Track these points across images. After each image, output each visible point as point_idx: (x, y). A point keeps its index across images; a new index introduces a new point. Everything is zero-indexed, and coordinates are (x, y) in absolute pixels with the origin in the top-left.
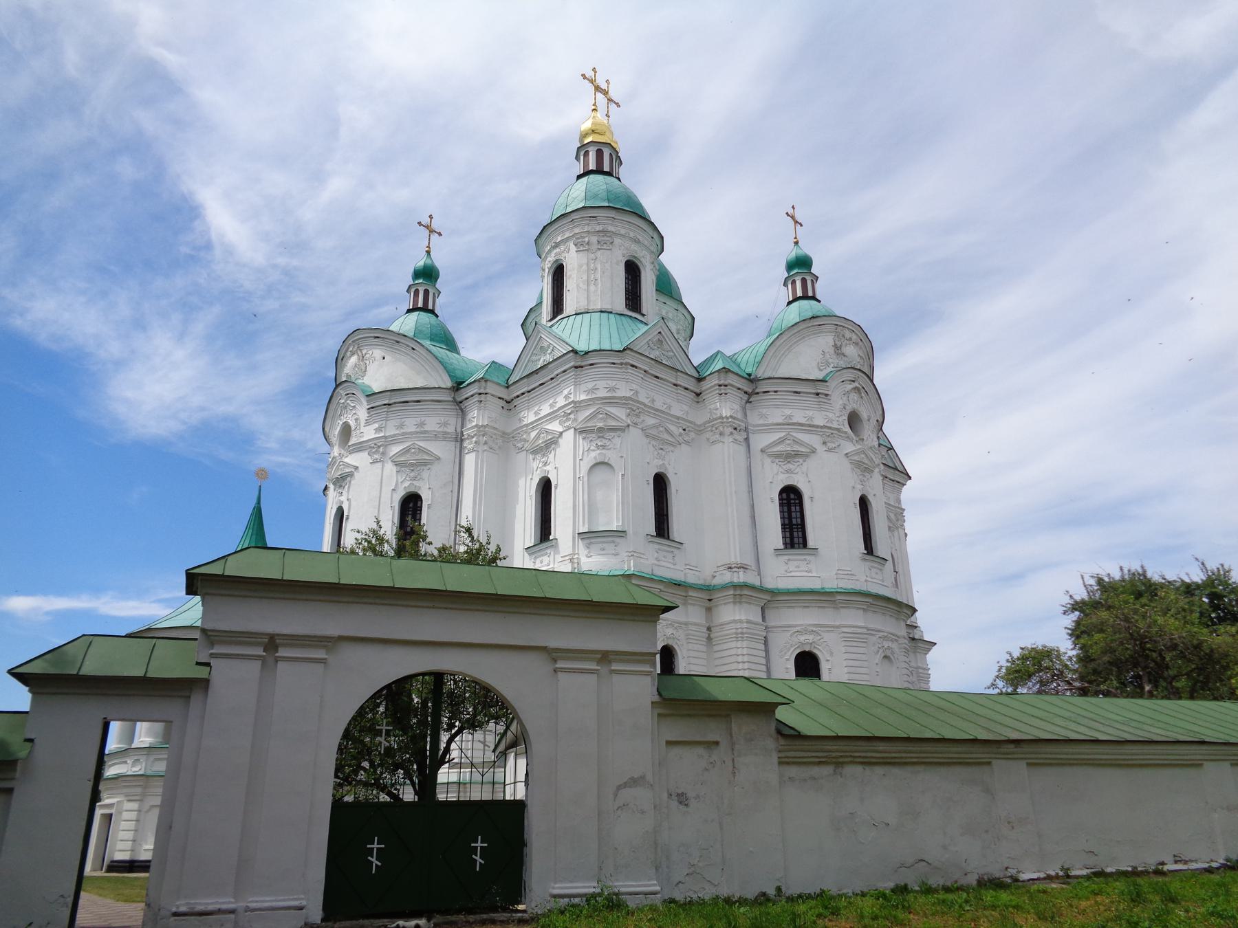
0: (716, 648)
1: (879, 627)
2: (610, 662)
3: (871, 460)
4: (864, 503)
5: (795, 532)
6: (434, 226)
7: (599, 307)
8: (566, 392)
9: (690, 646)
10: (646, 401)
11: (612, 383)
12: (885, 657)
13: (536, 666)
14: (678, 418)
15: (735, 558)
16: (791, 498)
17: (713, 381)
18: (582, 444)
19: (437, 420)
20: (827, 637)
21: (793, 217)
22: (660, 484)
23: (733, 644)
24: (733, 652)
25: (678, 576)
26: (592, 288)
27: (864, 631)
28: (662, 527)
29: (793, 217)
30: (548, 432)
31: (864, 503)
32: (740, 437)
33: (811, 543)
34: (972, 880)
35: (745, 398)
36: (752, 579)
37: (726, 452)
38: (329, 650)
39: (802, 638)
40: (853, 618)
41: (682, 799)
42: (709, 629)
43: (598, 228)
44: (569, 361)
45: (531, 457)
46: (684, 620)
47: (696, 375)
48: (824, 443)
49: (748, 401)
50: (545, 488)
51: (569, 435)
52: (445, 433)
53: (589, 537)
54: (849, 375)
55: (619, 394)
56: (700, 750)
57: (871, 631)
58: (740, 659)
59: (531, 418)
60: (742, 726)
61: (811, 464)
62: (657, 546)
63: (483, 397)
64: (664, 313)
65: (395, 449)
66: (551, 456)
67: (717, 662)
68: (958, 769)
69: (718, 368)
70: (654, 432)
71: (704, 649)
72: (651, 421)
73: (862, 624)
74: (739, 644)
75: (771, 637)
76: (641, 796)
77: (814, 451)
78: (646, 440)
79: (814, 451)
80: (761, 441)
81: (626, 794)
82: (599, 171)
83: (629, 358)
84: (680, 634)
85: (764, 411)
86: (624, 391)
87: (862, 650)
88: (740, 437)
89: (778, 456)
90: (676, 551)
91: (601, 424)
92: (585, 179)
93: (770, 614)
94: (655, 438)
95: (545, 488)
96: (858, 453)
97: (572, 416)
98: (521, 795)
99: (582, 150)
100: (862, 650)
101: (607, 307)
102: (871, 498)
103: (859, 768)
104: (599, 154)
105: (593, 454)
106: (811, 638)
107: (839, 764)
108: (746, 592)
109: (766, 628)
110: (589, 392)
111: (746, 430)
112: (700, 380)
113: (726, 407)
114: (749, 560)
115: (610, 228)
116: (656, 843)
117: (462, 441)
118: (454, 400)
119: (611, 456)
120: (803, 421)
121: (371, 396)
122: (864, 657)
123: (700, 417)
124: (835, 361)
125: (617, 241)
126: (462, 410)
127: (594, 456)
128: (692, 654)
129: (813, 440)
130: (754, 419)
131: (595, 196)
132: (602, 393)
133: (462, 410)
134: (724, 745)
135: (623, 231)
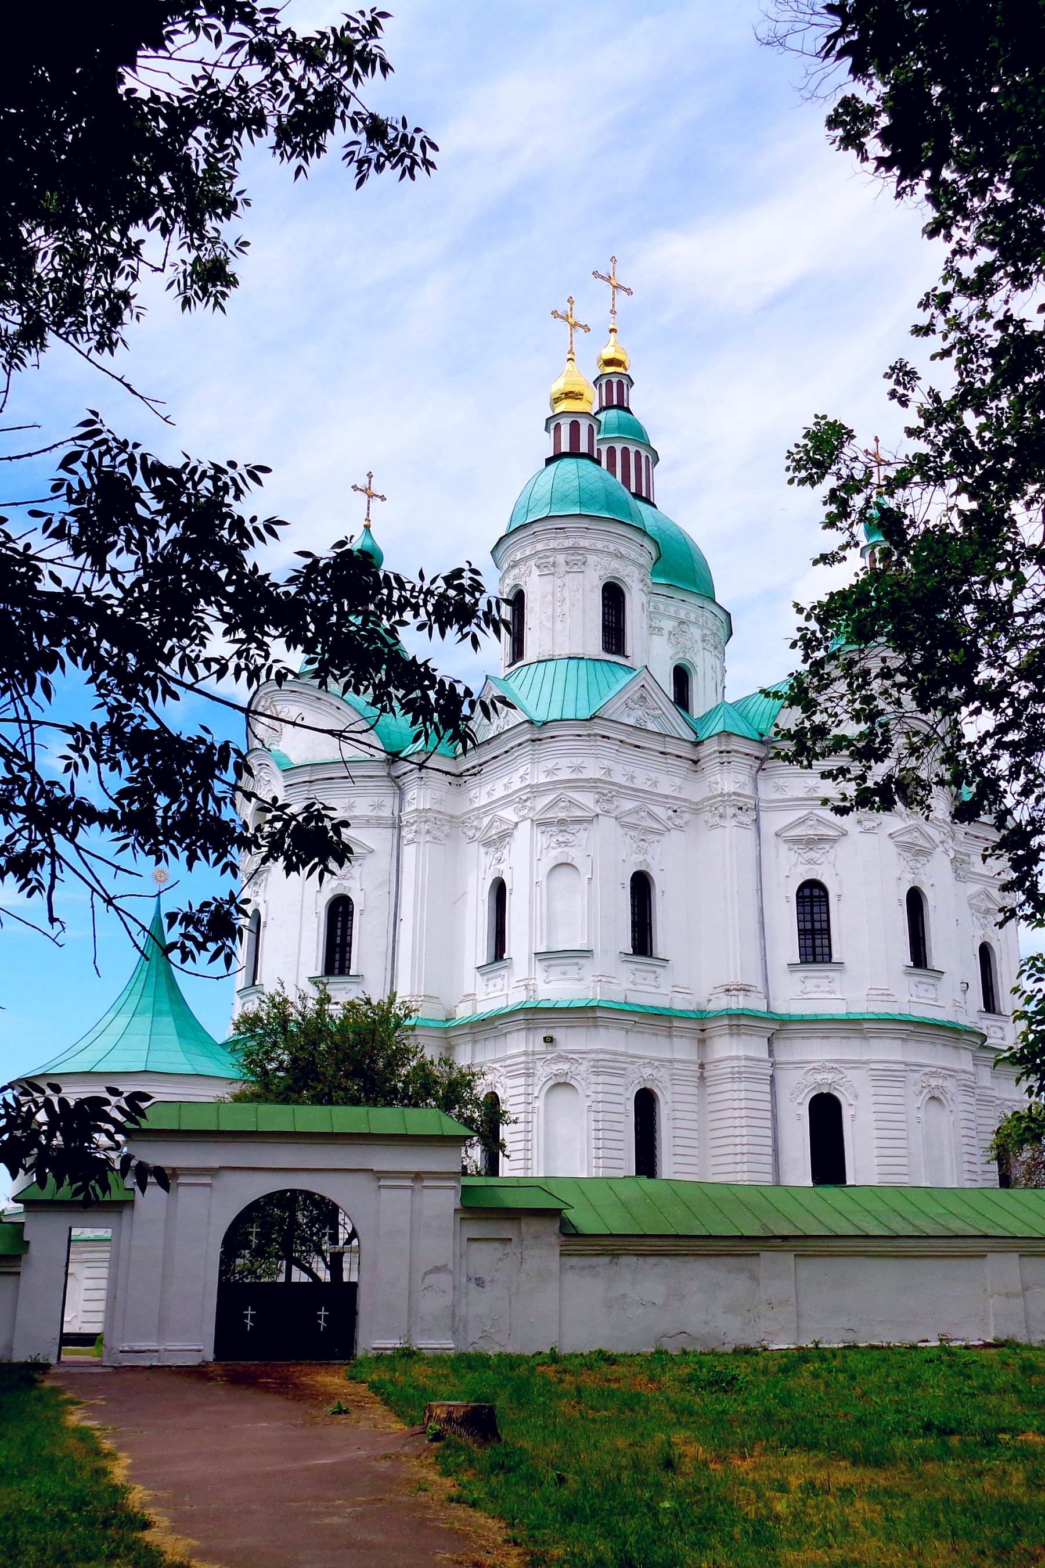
0: (710, 1090)
1: (923, 1061)
2: (422, 1179)
3: (929, 839)
4: (915, 900)
5: (815, 942)
6: (375, 489)
7: (566, 652)
8: (522, 771)
9: (676, 1089)
10: (622, 781)
11: (576, 761)
12: (933, 1098)
13: (363, 1182)
14: (667, 797)
15: (734, 978)
16: (812, 897)
17: (710, 748)
18: (542, 839)
19: (369, 800)
20: (852, 1075)
22: (641, 886)
23: (729, 1086)
24: (728, 1096)
25: (660, 1001)
26: (559, 626)
27: (902, 1067)
28: (642, 941)
30: (501, 820)
31: (915, 900)
32: (747, 818)
33: (835, 958)
34: (729, 1348)
35: (757, 764)
36: (755, 1003)
37: (730, 839)
38: (212, 1176)
39: (819, 1077)
40: (887, 1051)
41: (480, 1282)
42: (702, 1066)
43: (568, 543)
44: (522, 733)
45: (482, 850)
46: (669, 1056)
47: (692, 738)
48: (859, 822)
49: (761, 769)
50: (499, 890)
51: (525, 827)
52: (379, 818)
53: (547, 956)
55: (586, 775)
56: (497, 1245)
57: (912, 1067)
58: (736, 1104)
59: (484, 800)
60: (530, 1227)
61: (842, 848)
62: (633, 966)
64: (682, 615)
66: (506, 851)
67: (712, 1107)
68: (728, 1260)
69: (719, 728)
70: (632, 819)
71: (695, 1091)
72: (628, 805)
73: (900, 1058)
74: (736, 1086)
75: (780, 1075)
76: (444, 1280)
77: (845, 834)
78: (621, 832)
79: (845, 834)
80: (774, 821)
81: (431, 1279)
82: (574, 453)
84: (663, 1074)
85: (781, 782)
86: (593, 771)
87: (897, 1091)
88: (747, 818)
89: (797, 841)
90: (658, 970)
91: (562, 815)
92: (553, 466)
93: (779, 1046)
94: (634, 827)
95: (499, 890)
96: (908, 831)
97: (528, 803)
98: (354, 1279)
99: (552, 424)
100: (897, 1091)
101: (577, 651)
102: (926, 890)
103: (634, 1258)
104: (575, 427)
105: (553, 853)
106: (829, 1077)
107: (614, 1255)
108: (743, 1022)
109: (773, 1065)
110: (549, 772)
111: (756, 808)
112: (697, 744)
113: (729, 779)
114: (754, 979)
115: (584, 543)
116: (453, 1314)
117: (400, 828)
118: (389, 775)
119: (574, 854)
121: (289, 770)
122: (899, 1100)
123: (695, 792)
125: (592, 558)
126: (400, 788)
127: (555, 855)
128: (677, 1098)
130: (767, 791)
131: (564, 498)
132: (565, 775)
133: (400, 788)
134: (515, 1240)
135: (599, 545)
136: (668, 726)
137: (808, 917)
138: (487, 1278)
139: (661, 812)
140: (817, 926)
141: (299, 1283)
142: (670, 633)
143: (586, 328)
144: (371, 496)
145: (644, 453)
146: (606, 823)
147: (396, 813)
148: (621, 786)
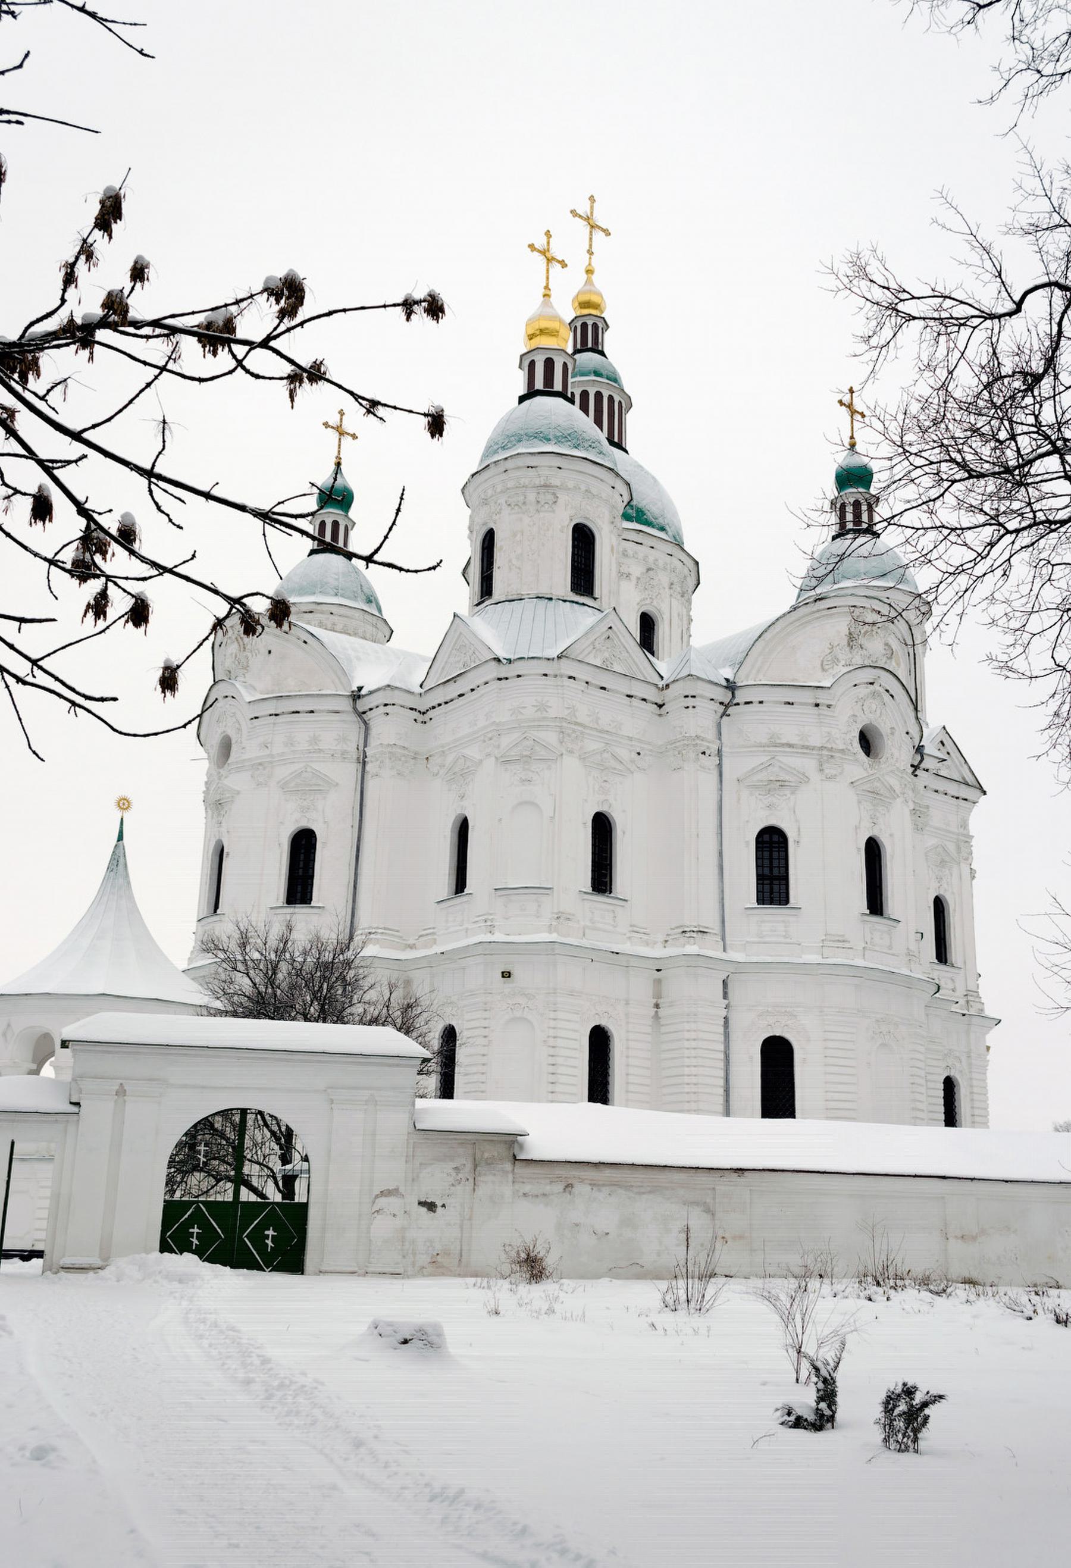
0: (663, 1029)
3: (891, 789)
4: (873, 851)
21: (850, 406)
29: (850, 406)
31: (873, 851)
41: (431, 1206)
49: (724, 714)
51: (490, 764)
54: (869, 675)
55: (552, 713)
63: (388, 709)
65: (282, 772)
71: (649, 1030)
77: (807, 779)
81: (382, 1202)
83: (567, 667)
92: (527, 403)
101: (544, 591)
111: (719, 752)
120: (794, 740)
124: (844, 655)
126: (365, 723)
129: (808, 765)
133: (365, 723)
136: (634, 668)
137: (767, 862)
138: (439, 1203)
139: (625, 754)
140: (776, 872)
141: (248, 1202)
142: (638, 579)
143: (563, 264)
144: (342, 433)
145: (617, 399)
146: (571, 763)
147: (361, 748)
148: (585, 727)
